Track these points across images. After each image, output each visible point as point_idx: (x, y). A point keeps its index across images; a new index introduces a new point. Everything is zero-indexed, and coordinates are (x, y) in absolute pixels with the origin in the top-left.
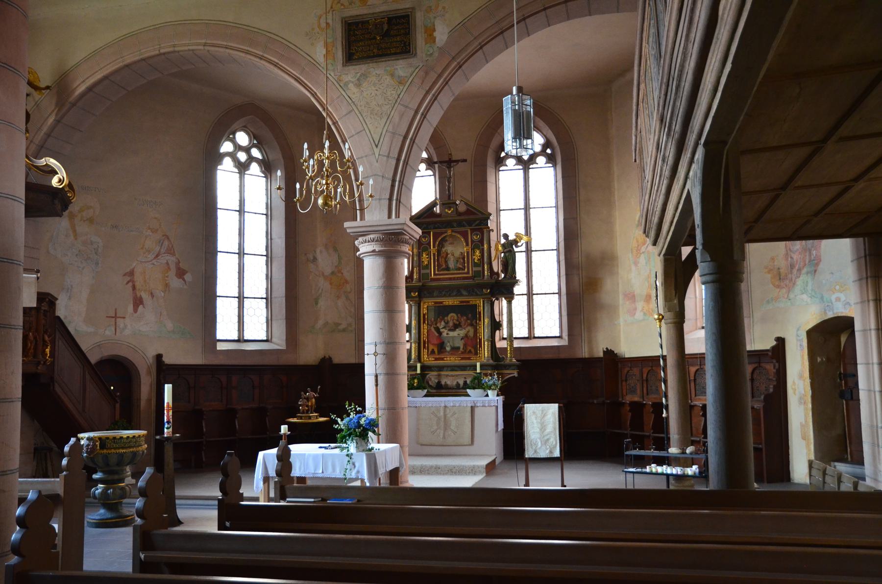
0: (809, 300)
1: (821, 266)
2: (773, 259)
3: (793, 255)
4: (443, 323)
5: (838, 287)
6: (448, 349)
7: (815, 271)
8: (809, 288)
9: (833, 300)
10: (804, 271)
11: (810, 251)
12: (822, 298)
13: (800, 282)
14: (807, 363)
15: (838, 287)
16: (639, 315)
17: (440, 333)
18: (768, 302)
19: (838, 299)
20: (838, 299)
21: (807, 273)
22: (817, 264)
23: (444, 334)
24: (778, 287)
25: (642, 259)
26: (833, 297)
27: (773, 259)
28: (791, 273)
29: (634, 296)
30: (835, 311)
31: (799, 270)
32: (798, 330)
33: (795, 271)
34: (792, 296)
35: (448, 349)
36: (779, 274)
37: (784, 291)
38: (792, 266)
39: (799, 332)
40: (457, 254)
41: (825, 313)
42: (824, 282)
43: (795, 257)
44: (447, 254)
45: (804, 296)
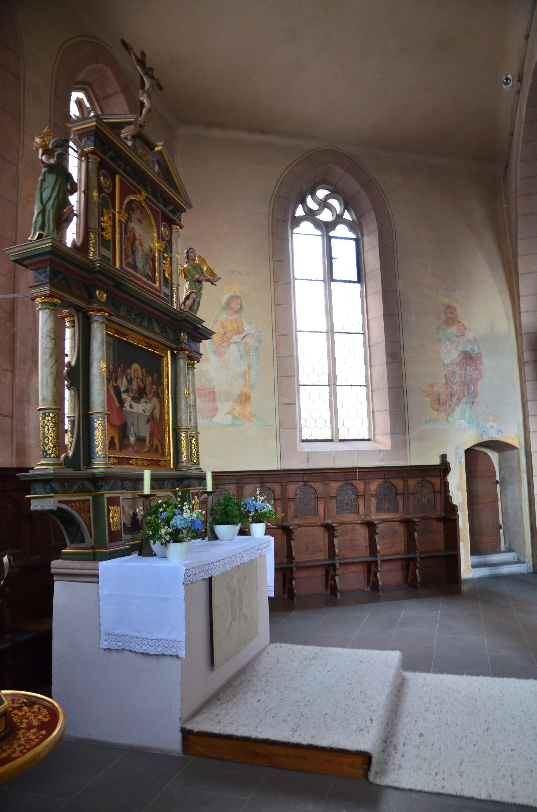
0: (466, 425)
1: (478, 399)
2: (432, 385)
3: (452, 386)
4: (124, 380)
5: (491, 418)
6: (132, 439)
7: (473, 402)
8: (467, 414)
9: (488, 427)
10: (464, 400)
11: (469, 386)
12: (478, 424)
13: (458, 409)
14: (464, 477)
15: (491, 418)
16: (219, 418)
17: (122, 402)
18: (426, 422)
19: (492, 427)
20: (492, 427)
21: (466, 403)
22: (475, 397)
23: (127, 405)
24: (438, 410)
25: (233, 351)
26: (488, 425)
27: (432, 385)
28: (451, 400)
29: (214, 393)
30: (490, 436)
31: (459, 399)
32: (457, 449)
33: (454, 399)
34: (450, 419)
35: (132, 439)
36: (439, 399)
37: (443, 414)
38: (452, 395)
39: (458, 451)
40: (146, 247)
41: (482, 437)
42: (480, 412)
43: (455, 388)
44: (135, 239)
45: (463, 421)
